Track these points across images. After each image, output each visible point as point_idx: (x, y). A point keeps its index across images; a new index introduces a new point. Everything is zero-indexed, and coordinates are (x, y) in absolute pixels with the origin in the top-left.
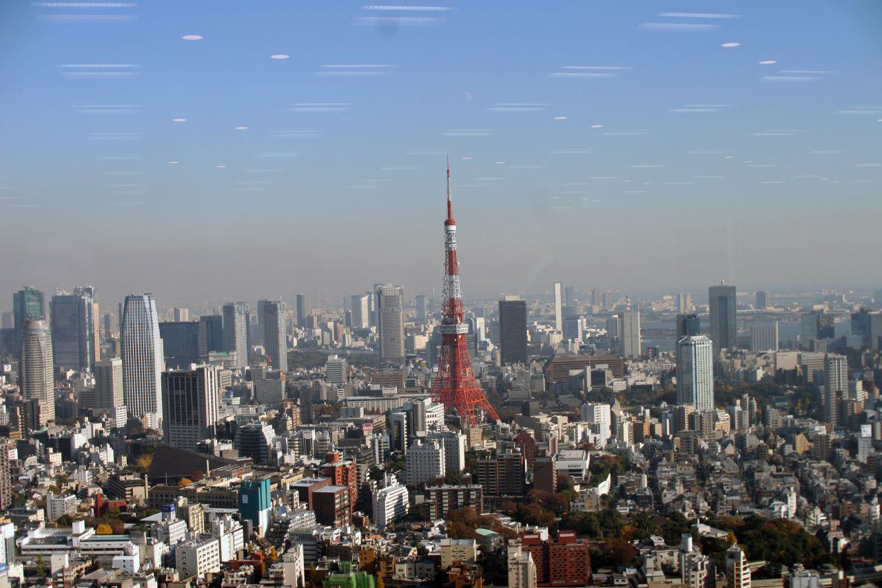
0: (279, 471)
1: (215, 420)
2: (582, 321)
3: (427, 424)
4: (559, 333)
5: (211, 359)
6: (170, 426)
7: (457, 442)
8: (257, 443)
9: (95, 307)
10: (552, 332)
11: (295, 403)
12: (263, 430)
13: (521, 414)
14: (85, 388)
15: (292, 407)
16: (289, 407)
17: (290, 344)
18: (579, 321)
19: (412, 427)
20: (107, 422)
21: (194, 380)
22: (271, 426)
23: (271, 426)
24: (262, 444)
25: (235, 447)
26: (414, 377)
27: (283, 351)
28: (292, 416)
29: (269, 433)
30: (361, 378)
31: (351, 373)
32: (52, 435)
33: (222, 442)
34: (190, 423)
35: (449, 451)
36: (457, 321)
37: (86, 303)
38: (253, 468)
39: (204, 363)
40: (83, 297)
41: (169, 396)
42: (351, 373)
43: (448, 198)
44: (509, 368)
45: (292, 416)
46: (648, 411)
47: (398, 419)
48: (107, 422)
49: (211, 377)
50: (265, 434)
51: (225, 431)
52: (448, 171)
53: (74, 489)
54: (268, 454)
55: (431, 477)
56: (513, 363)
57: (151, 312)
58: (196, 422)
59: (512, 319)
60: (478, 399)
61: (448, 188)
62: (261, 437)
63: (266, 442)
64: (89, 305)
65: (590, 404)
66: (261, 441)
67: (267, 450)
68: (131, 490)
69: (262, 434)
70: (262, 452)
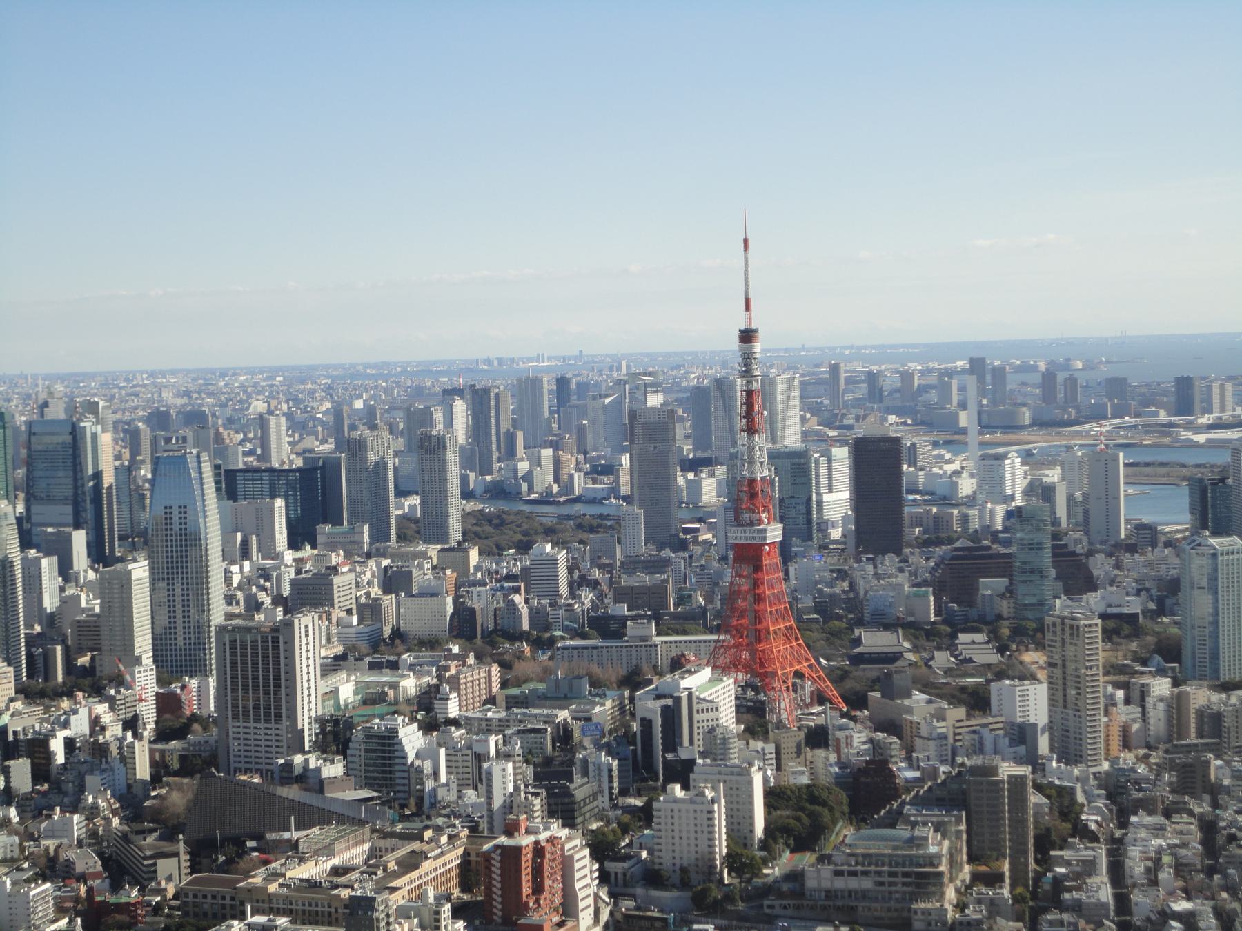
0: (422, 840)
1: (313, 714)
2: (1013, 462)
3: (701, 724)
4: (972, 476)
5: (320, 539)
6: (231, 723)
7: (750, 783)
8: (390, 772)
9: (106, 439)
10: (957, 473)
11: (464, 664)
12: (401, 735)
13: (878, 694)
14: (84, 610)
15: (459, 672)
16: (453, 671)
17: (467, 495)
18: (1007, 462)
19: (672, 741)
20: (118, 697)
21: (276, 641)
22: (416, 725)
23: (416, 725)
24: (397, 761)
25: (347, 774)
26: (691, 590)
27: (456, 507)
28: (458, 690)
29: (411, 739)
30: (595, 585)
31: (577, 573)
32: (15, 733)
33: (325, 760)
34: (267, 720)
35: (735, 813)
36: (760, 522)
37: (89, 435)
38: (374, 831)
39: (308, 547)
40: (82, 424)
41: (228, 647)
42: (577, 573)
43: (747, 293)
44: (870, 568)
45: (458, 690)
46: (1120, 694)
47: (648, 716)
48: (118, 697)
49: (307, 636)
50: (404, 742)
51: (335, 735)
52: (746, 241)
53: (52, 853)
54: (409, 778)
55: (698, 856)
56: (877, 554)
57: (202, 484)
58: (278, 716)
59: (878, 466)
60: (800, 663)
61: (746, 270)
62: (396, 747)
63: (405, 757)
64: (94, 437)
65: (1008, 682)
66: (397, 761)
67: (408, 771)
68: (155, 864)
69: (400, 743)
70: (398, 781)
